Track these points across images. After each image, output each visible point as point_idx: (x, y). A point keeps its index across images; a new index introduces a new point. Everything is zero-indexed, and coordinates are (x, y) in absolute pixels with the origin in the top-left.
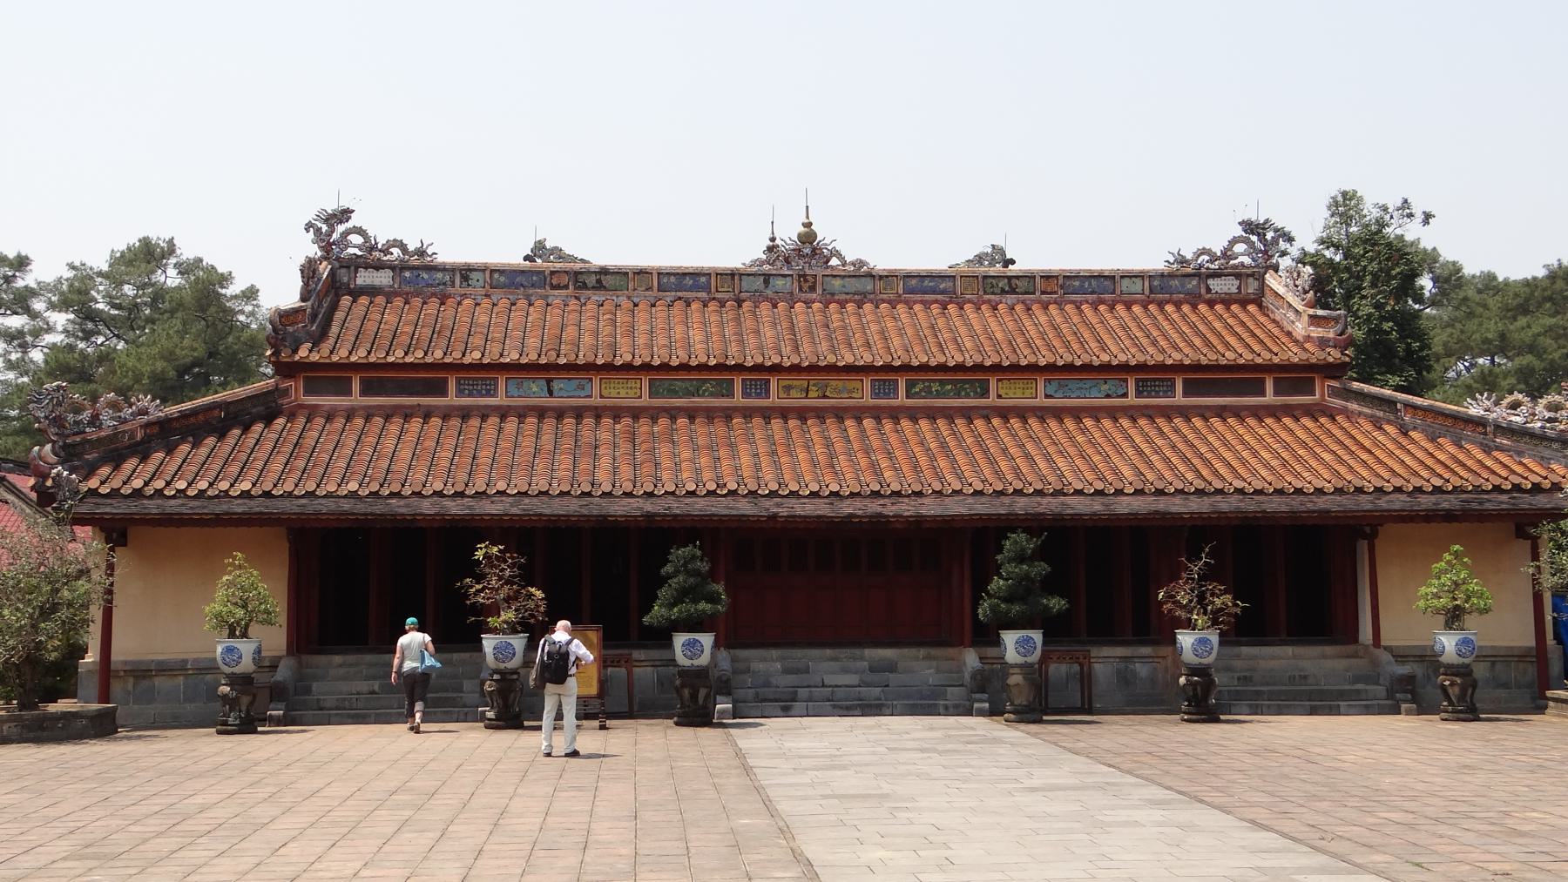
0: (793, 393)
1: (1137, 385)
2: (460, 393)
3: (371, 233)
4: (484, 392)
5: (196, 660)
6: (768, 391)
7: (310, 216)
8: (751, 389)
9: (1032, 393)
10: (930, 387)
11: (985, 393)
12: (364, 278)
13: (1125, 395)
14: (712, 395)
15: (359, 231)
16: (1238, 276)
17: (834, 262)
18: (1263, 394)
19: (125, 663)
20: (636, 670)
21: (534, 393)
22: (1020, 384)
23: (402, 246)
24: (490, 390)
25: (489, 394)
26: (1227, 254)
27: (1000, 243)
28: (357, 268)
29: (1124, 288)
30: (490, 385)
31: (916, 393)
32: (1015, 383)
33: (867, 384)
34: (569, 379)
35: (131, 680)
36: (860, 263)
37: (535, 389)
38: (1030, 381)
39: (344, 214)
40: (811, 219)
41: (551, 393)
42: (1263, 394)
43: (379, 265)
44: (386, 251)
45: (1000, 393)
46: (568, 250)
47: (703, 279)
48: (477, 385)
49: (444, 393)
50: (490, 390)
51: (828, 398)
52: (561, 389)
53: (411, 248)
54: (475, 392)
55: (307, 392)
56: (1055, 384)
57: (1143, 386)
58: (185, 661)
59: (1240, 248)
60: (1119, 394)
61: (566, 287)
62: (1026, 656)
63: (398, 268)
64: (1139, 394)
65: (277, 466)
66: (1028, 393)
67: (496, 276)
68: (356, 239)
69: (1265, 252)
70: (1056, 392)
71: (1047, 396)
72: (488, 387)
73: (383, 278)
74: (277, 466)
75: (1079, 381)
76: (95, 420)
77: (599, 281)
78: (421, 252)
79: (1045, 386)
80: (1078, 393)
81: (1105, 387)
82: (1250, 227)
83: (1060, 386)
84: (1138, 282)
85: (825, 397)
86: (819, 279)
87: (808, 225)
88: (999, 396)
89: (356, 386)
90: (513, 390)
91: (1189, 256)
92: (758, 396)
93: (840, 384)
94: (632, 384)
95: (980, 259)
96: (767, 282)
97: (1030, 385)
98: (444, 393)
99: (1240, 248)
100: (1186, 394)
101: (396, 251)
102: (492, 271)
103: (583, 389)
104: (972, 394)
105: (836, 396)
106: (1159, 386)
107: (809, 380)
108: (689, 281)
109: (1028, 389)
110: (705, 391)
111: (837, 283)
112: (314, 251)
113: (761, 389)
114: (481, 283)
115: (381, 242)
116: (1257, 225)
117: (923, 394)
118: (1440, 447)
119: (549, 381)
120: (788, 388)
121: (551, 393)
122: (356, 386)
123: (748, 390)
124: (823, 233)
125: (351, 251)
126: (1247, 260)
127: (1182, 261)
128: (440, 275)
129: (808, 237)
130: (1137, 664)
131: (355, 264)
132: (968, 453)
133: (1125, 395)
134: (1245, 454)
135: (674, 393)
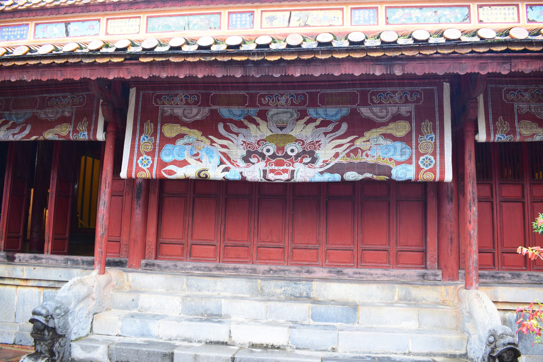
0: (276, 23)
4: (18, 37)
8: (236, 22)
9: (514, 19)
10: (410, 14)
21: (55, 35)
24: (23, 35)
30: (23, 31)
34: (83, 21)
38: (511, 7)
45: (480, 19)
48: (14, 31)
50: (23, 35)
51: (310, 26)
52: (76, 30)
54: (12, 37)
70: (538, 17)
71: (529, 21)
72: (22, 33)
79: (527, 12)
85: (306, 25)
97: (511, 11)
103: (93, 28)
104: (453, 20)
107: (291, 11)
109: (509, 14)
110: (195, 25)
113: (246, 21)
117: (403, 21)
123: (234, 23)
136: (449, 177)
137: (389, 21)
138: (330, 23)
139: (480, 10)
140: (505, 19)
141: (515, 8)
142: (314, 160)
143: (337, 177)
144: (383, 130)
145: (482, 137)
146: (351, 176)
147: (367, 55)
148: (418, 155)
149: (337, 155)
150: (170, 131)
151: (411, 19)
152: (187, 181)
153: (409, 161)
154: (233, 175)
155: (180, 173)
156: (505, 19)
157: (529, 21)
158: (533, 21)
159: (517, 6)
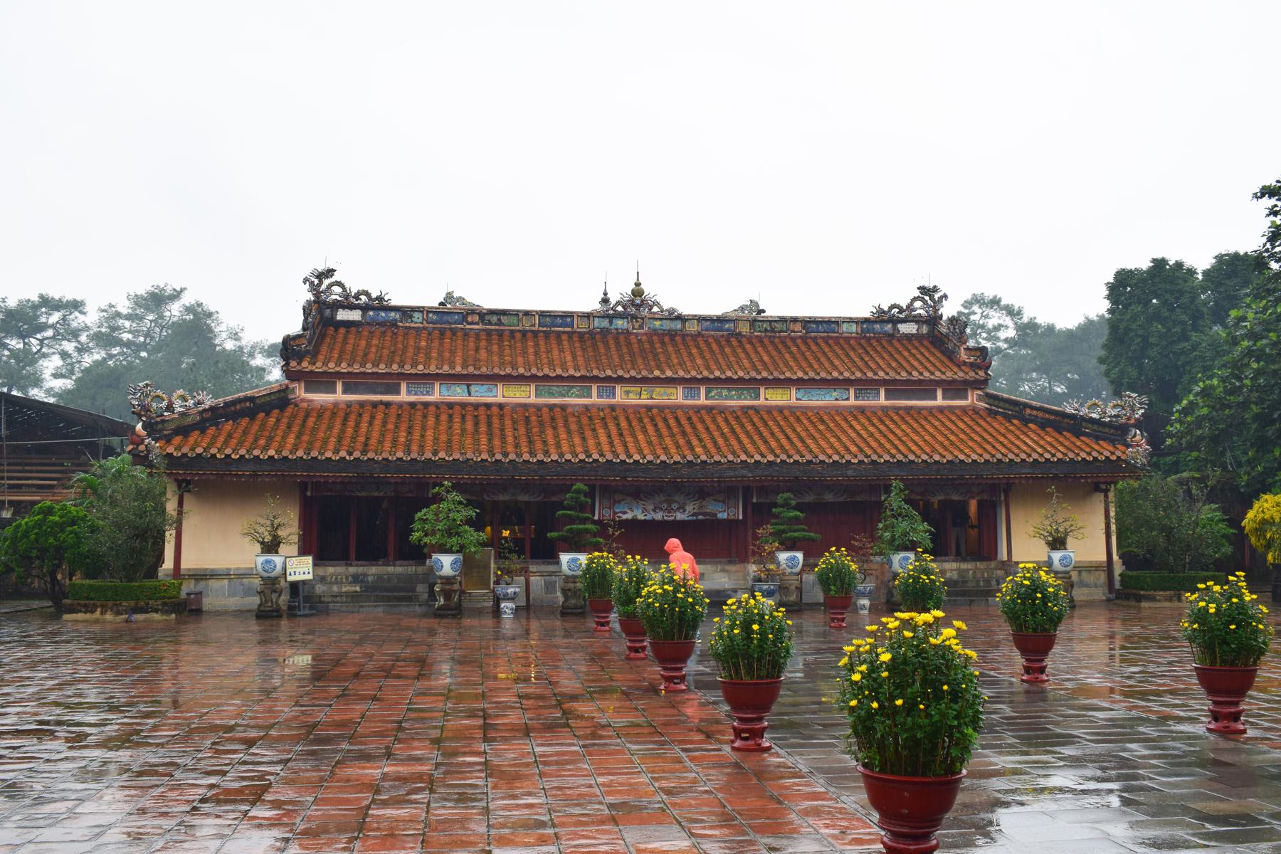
0: (631, 395)
1: (855, 393)
2: (409, 393)
3: (347, 286)
5: (237, 569)
6: (614, 394)
7: (306, 274)
11: (757, 397)
12: (342, 315)
13: (848, 399)
14: (577, 396)
15: (339, 284)
16: (917, 322)
17: (655, 309)
18: (935, 399)
19: (189, 570)
20: (532, 578)
22: (780, 391)
23: (367, 293)
25: (428, 393)
26: (910, 307)
27: (755, 299)
28: (338, 308)
29: (844, 329)
33: (680, 389)
35: (193, 581)
36: (672, 311)
37: (459, 391)
39: (330, 272)
40: (640, 281)
41: (470, 394)
42: (935, 399)
43: (352, 307)
44: (357, 297)
46: (469, 299)
47: (569, 320)
49: (398, 393)
53: (374, 296)
55: (307, 391)
56: (802, 391)
58: (229, 569)
59: (918, 304)
61: (477, 323)
63: (365, 309)
64: (857, 398)
65: (291, 440)
66: (785, 398)
67: (430, 315)
68: (337, 289)
69: (934, 307)
71: (797, 399)
73: (355, 316)
74: (291, 440)
76: (170, 407)
77: (499, 320)
78: (380, 298)
81: (835, 394)
82: (923, 290)
83: (806, 393)
84: (854, 326)
85: (652, 398)
86: (646, 320)
87: (638, 284)
88: (766, 399)
89: (339, 387)
90: (444, 391)
91: (886, 309)
92: (608, 397)
93: (662, 390)
94: (523, 388)
95: (742, 308)
96: (611, 322)
98: (398, 393)
99: (918, 304)
100: (887, 399)
101: (363, 298)
102: (428, 312)
108: (559, 321)
111: (658, 323)
112: (310, 297)
114: (420, 320)
115: (354, 291)
116: (929, 290)
118: (1047, 433)
119: (468, 386)
120: (627, 393)
121: (470, 394)
122: (339, 387)
124: (649, 290)
125: (334, 297)
126: (922, 312)
127: (881, 311)
128: (393, 314)
129: (638, 292)
131: (337, 305)
132: (748, 435)
133: (848, 399)
134: (927, 437)
135: (552, 395)
136: (741, 517)
142: (685, 511)
145: (755, 501)
146: (700, 517)
150: (617, 497)
152: (627, 520)
154: (649, 517)
155: (624, 517)
157: (797, 399)
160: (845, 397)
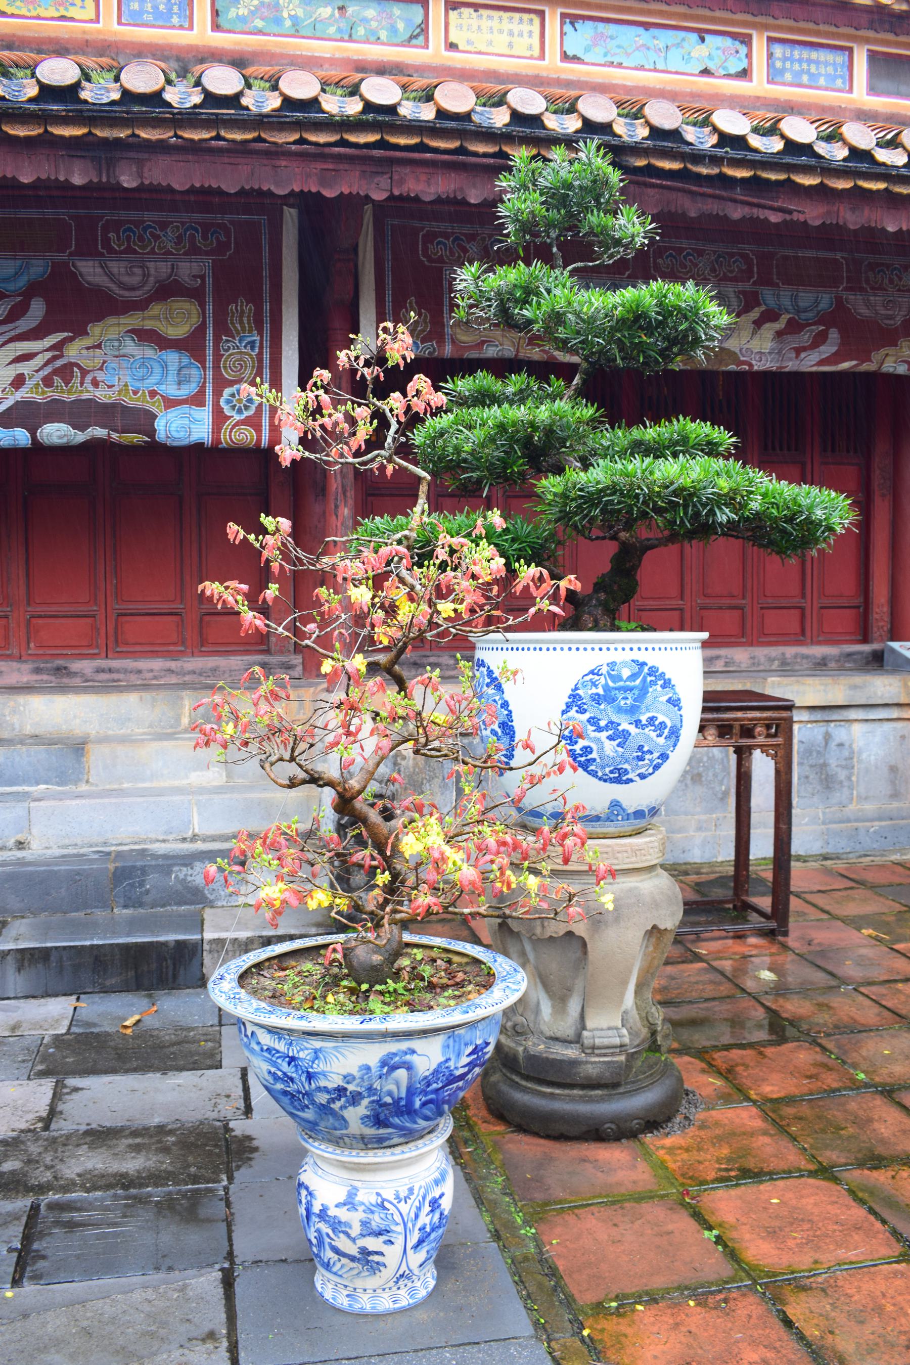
9: (530, 48)
13: (744, 74)
31: (241, 19)
32: (490, 17)
38: (526, 16)
45: (453, 38)
56: (586, 30)
57: (785, 59)
60: (732, 71)
62: (619, 777)
70: (587, 50)
71: (565, 57)
75: (641, 30)
79: (563, 34)
80: (638, 58)
97: (525, 28)
104: (383, 35)
105: (24, 12)
106: (817, 62)
109: (521, 34)
117: (259, 24)
130: (857, 728)
137: (221, 20)
138: (63, 12)
139: (453, 15)
140: (510, 45)
141: (537, 21)
143: (20, 437)
144: (133, 320)
147: (46, 131)
148: (220, 384)
149: (18, 382)
151: (278, 21)
153: (197, 400)
156: (510, 45)
157: (565, 57)
158: (576, 59)
159: (541, 14)
160: (735, 66)
